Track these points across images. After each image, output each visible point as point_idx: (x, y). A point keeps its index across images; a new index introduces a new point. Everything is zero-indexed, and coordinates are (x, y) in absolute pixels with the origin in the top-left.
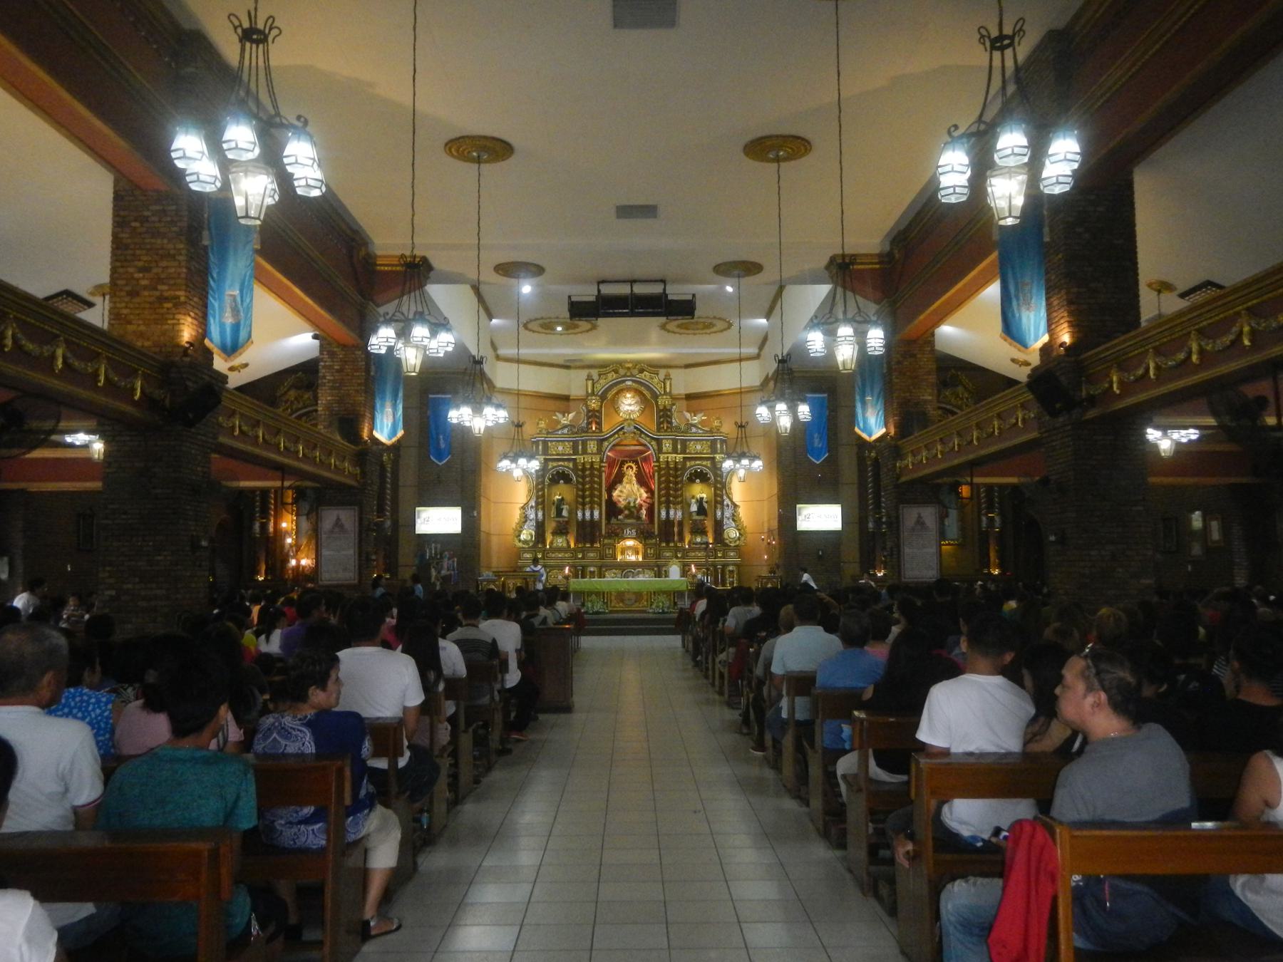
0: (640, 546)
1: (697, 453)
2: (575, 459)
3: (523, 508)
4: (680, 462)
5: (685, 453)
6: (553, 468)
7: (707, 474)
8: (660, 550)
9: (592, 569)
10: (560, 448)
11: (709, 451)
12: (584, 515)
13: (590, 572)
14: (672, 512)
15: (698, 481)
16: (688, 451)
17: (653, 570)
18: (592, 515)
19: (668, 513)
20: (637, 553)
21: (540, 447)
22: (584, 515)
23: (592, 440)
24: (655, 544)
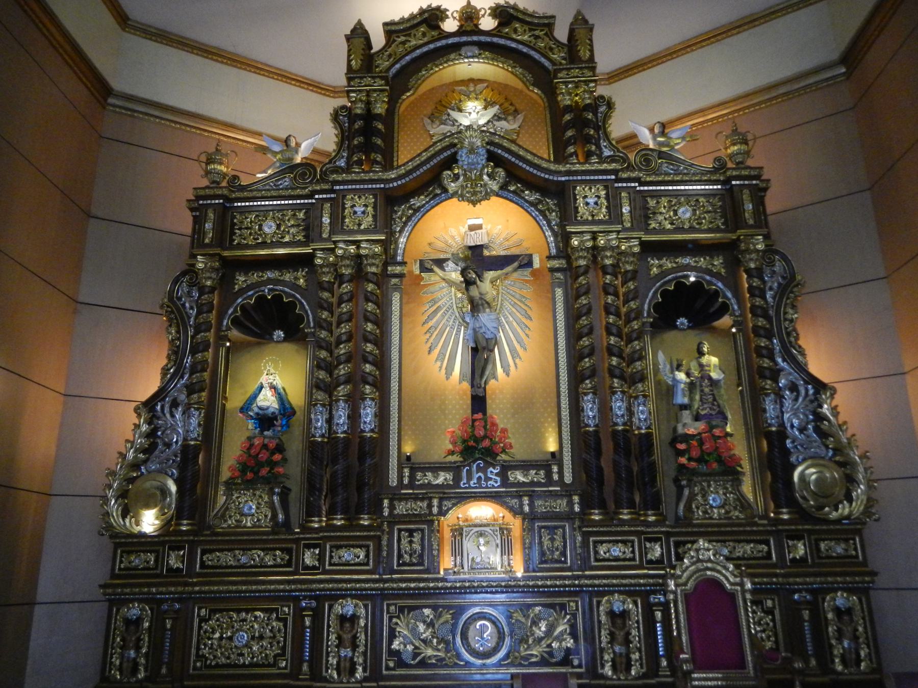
0: (516, 525)
1: (679, 230)
2: (311, 257)
3: (149, 404)
4: (634, 254)
5: (648, 231)
6: (242, 291)
7: (716, 293)
8: (586, 535)
9: (348, 607)
10: (269, 228)
11: (720, 223)
12: (330, 421)
13: (343, 619)
14: (618, 406)
15: (682, 321)
16: (653, 225)
17: (563, 607)
18: (354, 417)
19: (605, 410)
20: (506, 549)
21: (208, 226)
22: (330, 421)
23: (360, 193)
24: (569, 516)
